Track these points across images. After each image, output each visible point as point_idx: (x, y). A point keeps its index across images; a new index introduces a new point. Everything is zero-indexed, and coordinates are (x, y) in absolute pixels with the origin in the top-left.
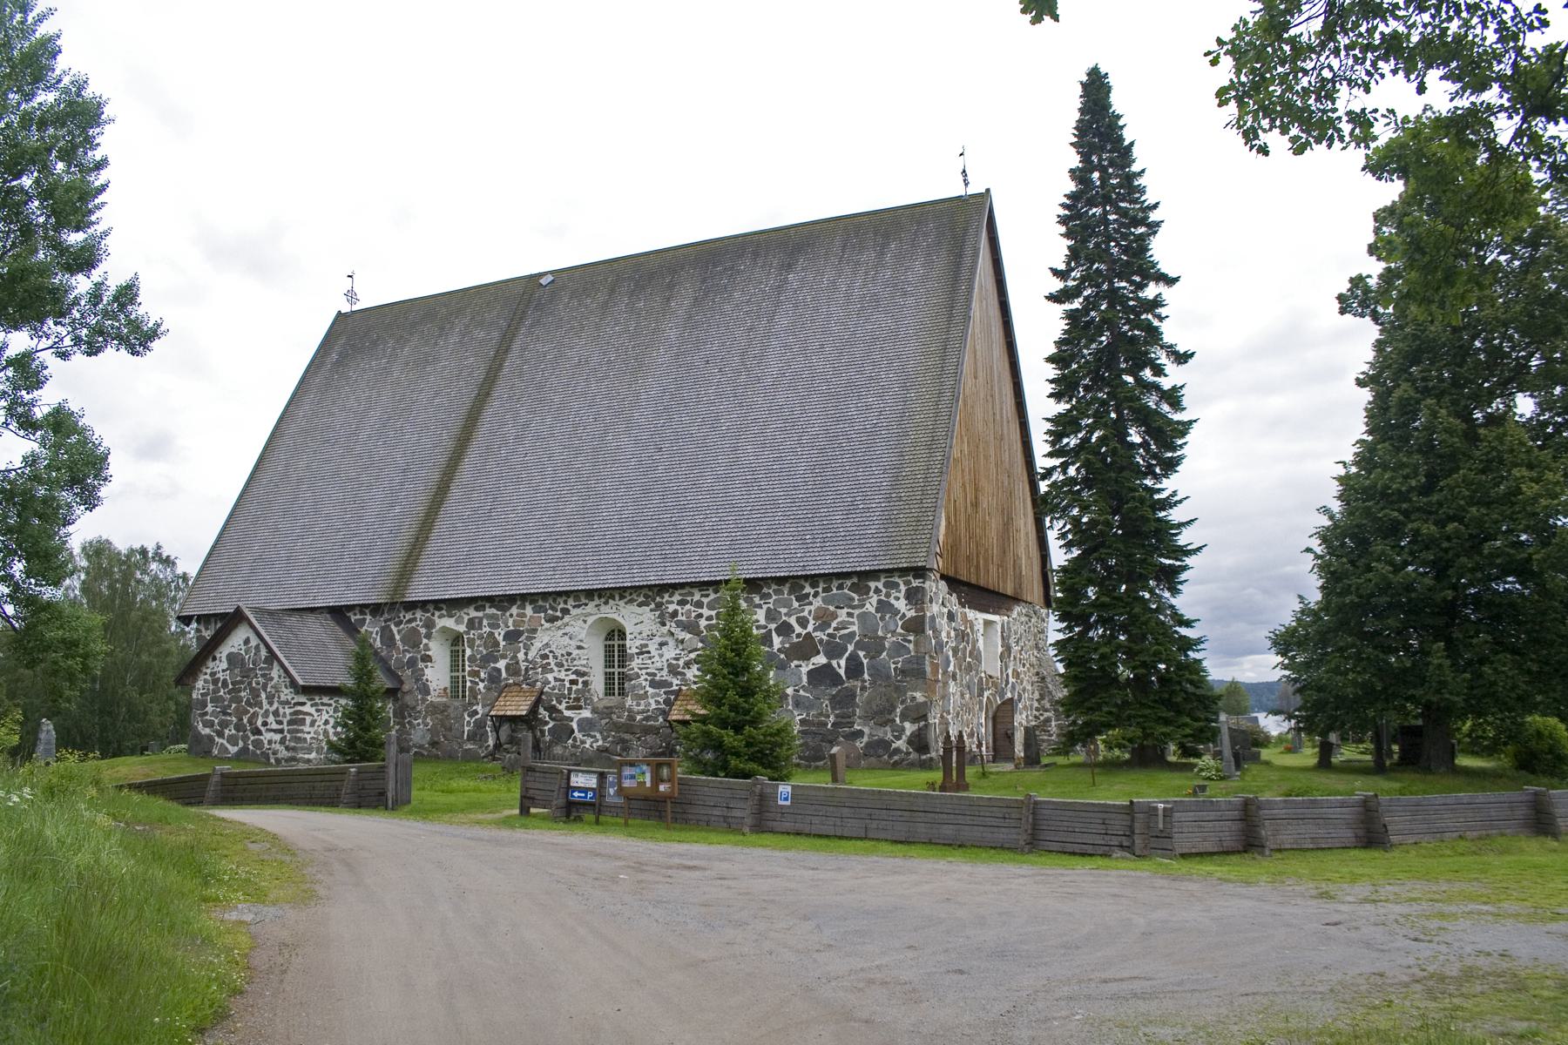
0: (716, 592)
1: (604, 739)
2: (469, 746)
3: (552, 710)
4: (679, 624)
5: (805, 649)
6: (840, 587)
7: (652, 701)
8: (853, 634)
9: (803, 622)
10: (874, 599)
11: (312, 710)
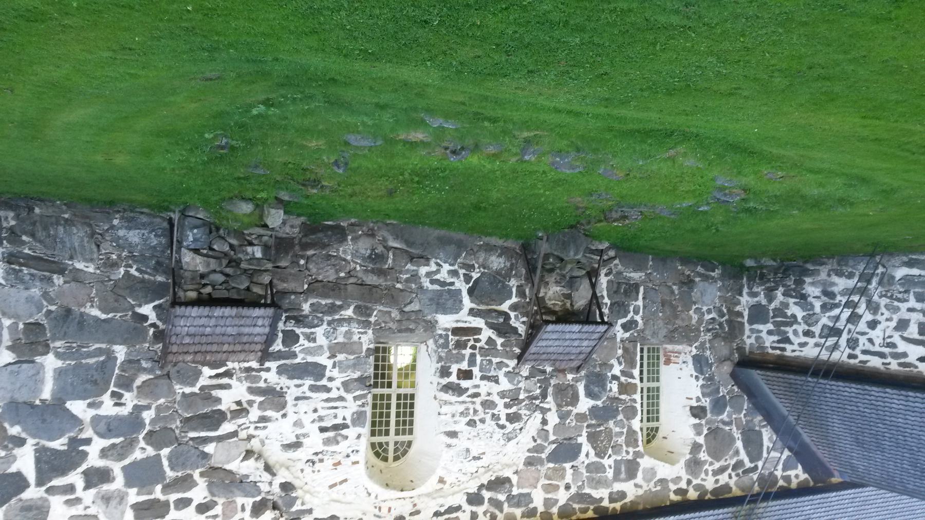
1: (415, 277)
2: (636, 276)
3: (504, 329)
7: (322, 340)
11: (902, 347)
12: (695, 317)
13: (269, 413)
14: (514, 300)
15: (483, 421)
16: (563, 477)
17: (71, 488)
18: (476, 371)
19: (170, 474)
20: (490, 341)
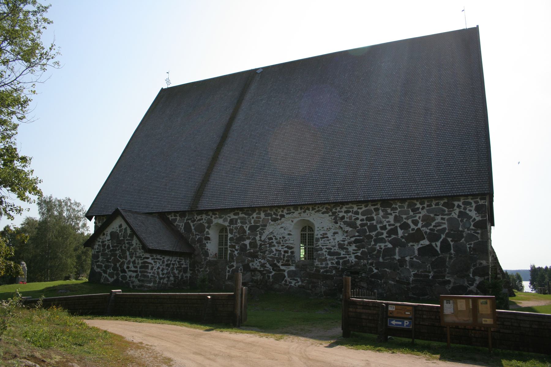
0: (366, 206)
1: (302, 281)
2: (229, 283)
4: (345, 223)
5: (417, 236)
8: (444, 229)
9: (415, 223)
10: (457, 211)
12: (207, 269)
13: (342, 243)
14: (271, 275)
15: (280, 238)
16: (254, 221)
17: (390, 225)
18: (283, 253)
19: (366, 227)
20: (279, 262)
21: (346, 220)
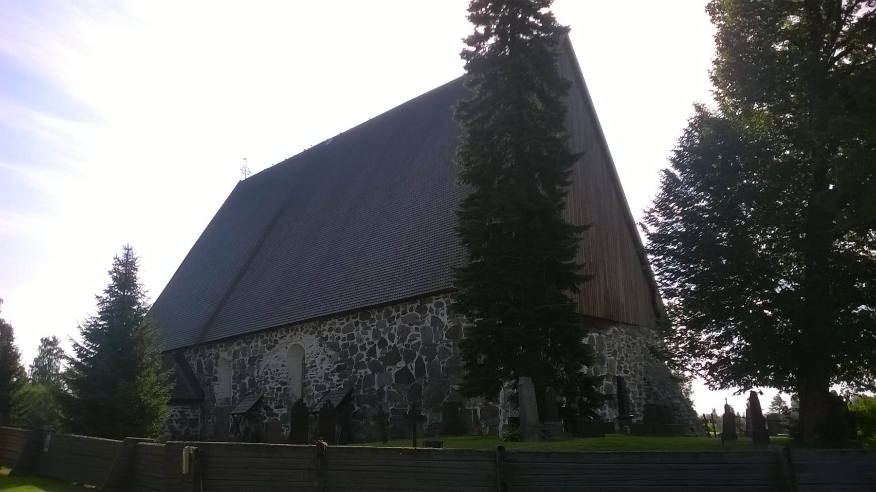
3: (268, 408)
4: (329, 344)
5: (392, 357)
6: (411, 310)
9: (392, 337)
10: (429, 317)
17: (369, 343)
21: (329, 340)
